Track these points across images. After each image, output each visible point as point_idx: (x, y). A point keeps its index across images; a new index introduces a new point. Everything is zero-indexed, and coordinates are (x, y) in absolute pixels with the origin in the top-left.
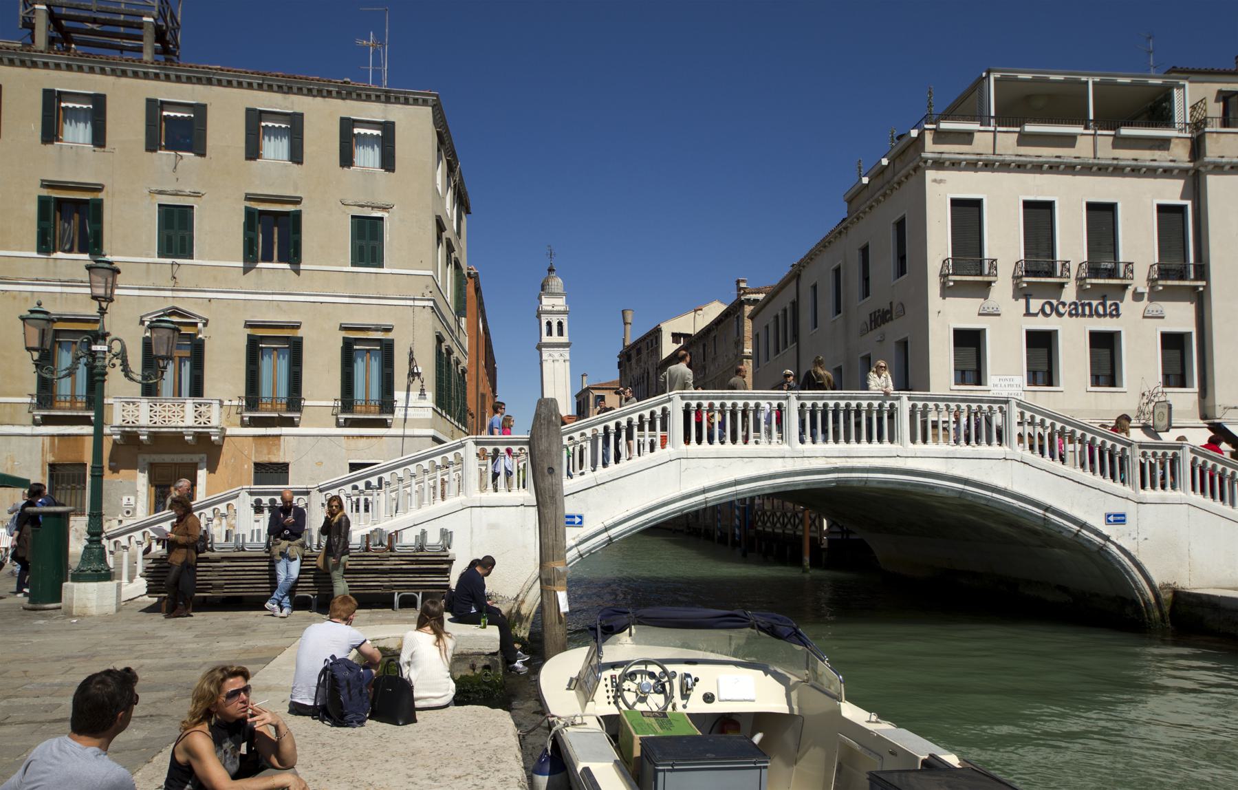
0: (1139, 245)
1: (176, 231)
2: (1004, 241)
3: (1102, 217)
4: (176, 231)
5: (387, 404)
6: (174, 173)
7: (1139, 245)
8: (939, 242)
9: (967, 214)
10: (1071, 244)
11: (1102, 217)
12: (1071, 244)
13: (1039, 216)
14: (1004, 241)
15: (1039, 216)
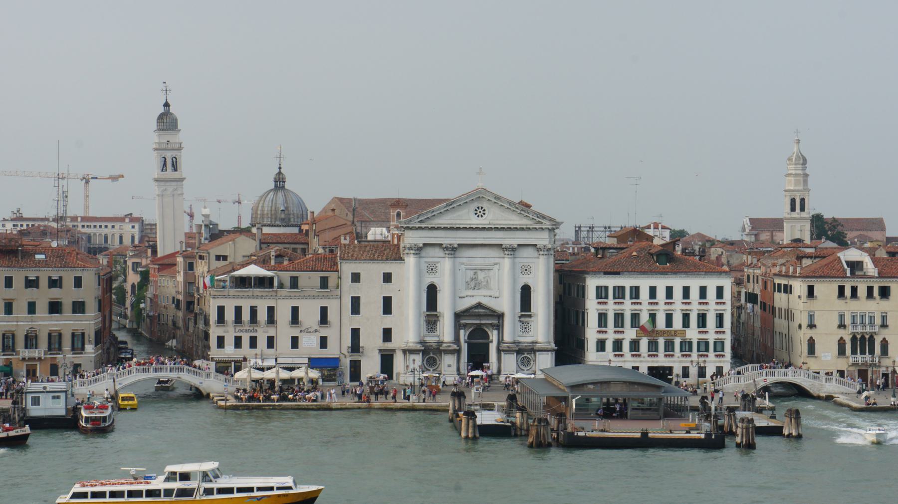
0: (262, 316)
1: (32, 308)
2: (230, 315)
3: (254, 311)
4: (32, 308)
5: (83, 349)
6: (31, 294)
7: (262, 316)
8: (213, 317)
9: (221, 310)
10: (246, 316)
11: (254, 311)
12: (246, 316)
13: (238, 310)
14: (230, 315)
15: (238, 310)
